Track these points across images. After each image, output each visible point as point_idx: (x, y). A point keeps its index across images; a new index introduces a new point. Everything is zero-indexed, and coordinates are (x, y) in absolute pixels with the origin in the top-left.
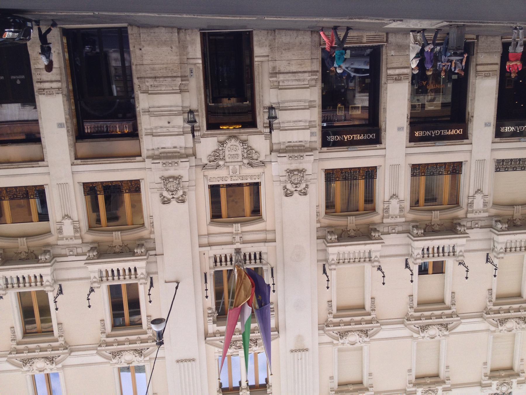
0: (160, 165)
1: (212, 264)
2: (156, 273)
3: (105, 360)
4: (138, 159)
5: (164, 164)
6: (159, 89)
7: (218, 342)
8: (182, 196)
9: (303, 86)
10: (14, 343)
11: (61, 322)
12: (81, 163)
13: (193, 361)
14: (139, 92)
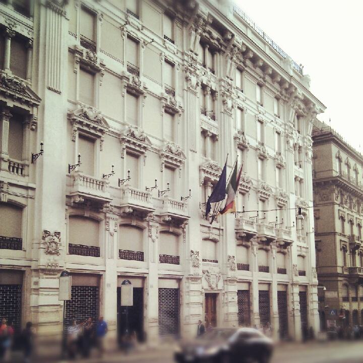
1: (26, 168)
2: (68, 176)
3: (107, 120)
7: (33, 97)
8: (46, 237)
10: (145, 155)
11: (122, 159)
13: (50, 88)
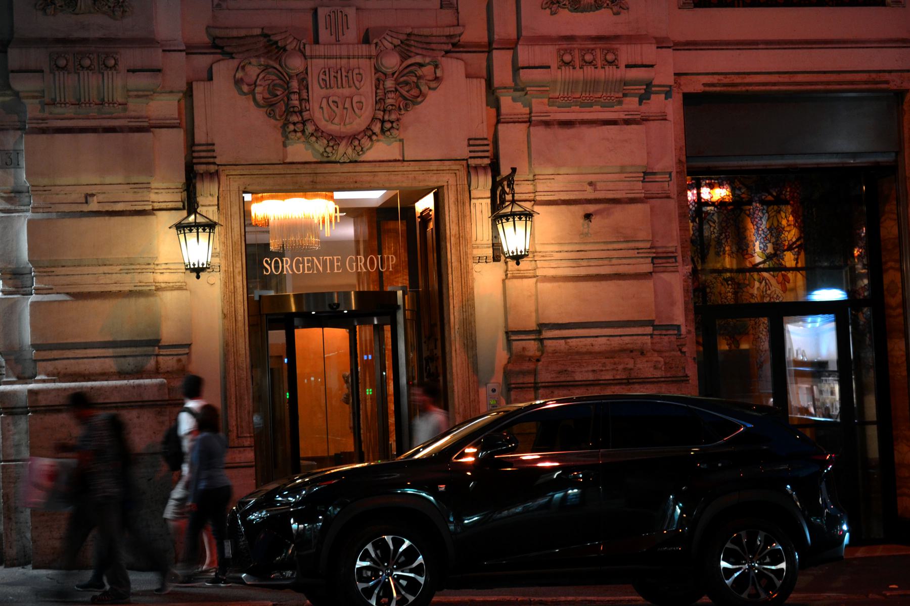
0: (623, 60)
4: (696, 86)
5: (610, 63)
6: (616, 342)
9: (55, 354)
12: (887, 76)
14: (683, 330)
